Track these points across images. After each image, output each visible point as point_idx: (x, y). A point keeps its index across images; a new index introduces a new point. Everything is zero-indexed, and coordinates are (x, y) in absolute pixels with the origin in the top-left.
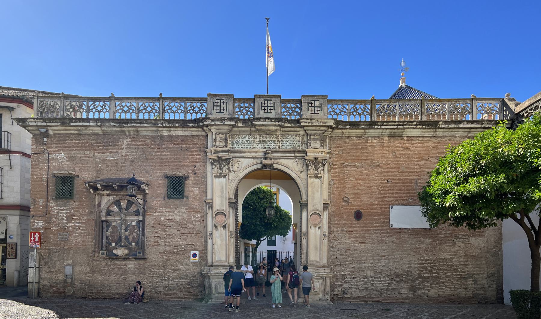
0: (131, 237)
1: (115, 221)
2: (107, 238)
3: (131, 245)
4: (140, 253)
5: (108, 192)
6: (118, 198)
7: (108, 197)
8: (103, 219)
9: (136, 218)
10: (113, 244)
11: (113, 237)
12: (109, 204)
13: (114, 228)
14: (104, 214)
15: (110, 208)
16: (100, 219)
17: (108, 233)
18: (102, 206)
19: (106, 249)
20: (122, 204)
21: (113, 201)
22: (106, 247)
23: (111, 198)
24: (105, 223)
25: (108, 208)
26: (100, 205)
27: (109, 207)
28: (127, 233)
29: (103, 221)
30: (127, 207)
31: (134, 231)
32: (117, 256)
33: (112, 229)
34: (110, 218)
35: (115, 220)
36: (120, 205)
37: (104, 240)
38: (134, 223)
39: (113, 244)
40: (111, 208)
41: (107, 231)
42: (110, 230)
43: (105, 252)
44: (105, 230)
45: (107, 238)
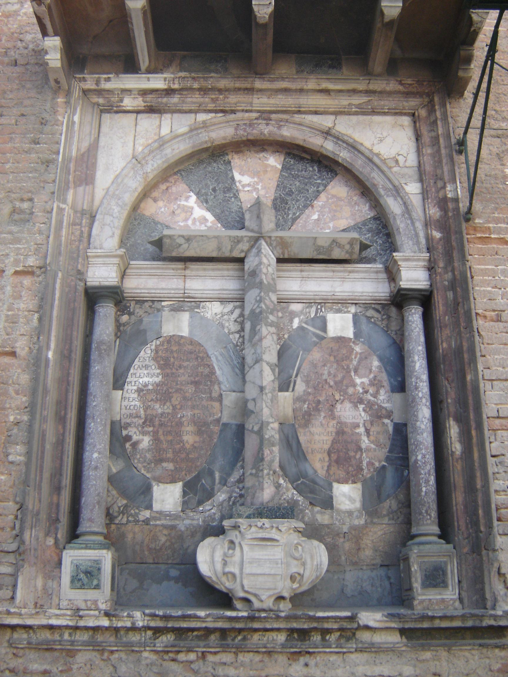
0: (318, 437)
1: (187, 303)
2: (118, 441)
3: (328, 503)
4: (435, 578)
5: (157, 82)
6: (222, 131)
7: (147, 123)
8: (102, 273)
9: (365, 284)
10: (167, 497)
11: (162, 428)
12: (154, 166)
13: (176, 355)
14: (107, 236)
15: (150, 208)
16: (81, 275)
17: (127, 401)
18: (103, 179)
19: (112, 540)
20: (242, 179)
21: (181, 148)
22: (110, 516)
23: (176, 131)
24: (106, 312)
25: (136, 207)
26: (85, 168)
27: (145, 194)
28: (286, 398)
29: (93, 297)
30: (280, 204)
31: (343, 385)
32: (225, 600)
33: (164, 362)
34: (147, 281)
35: (197, 308)
36: (230, 187)
37: (97, 453)
38: (340, 324)
39: (167, 497)
40: (157, 209)
41: (119, 382)
42: (144, 374)
43: (106, 558)
44: (102, 368)
45: (118, 441)
